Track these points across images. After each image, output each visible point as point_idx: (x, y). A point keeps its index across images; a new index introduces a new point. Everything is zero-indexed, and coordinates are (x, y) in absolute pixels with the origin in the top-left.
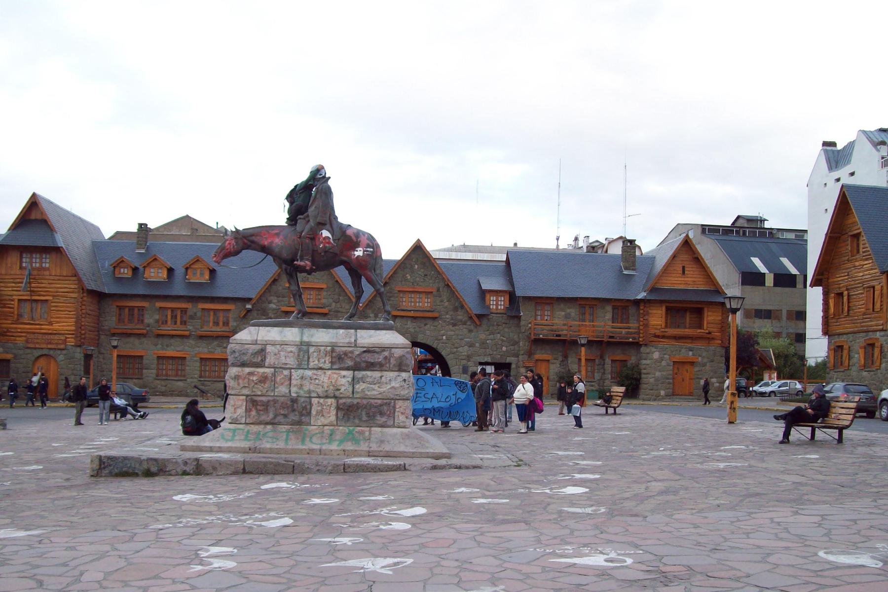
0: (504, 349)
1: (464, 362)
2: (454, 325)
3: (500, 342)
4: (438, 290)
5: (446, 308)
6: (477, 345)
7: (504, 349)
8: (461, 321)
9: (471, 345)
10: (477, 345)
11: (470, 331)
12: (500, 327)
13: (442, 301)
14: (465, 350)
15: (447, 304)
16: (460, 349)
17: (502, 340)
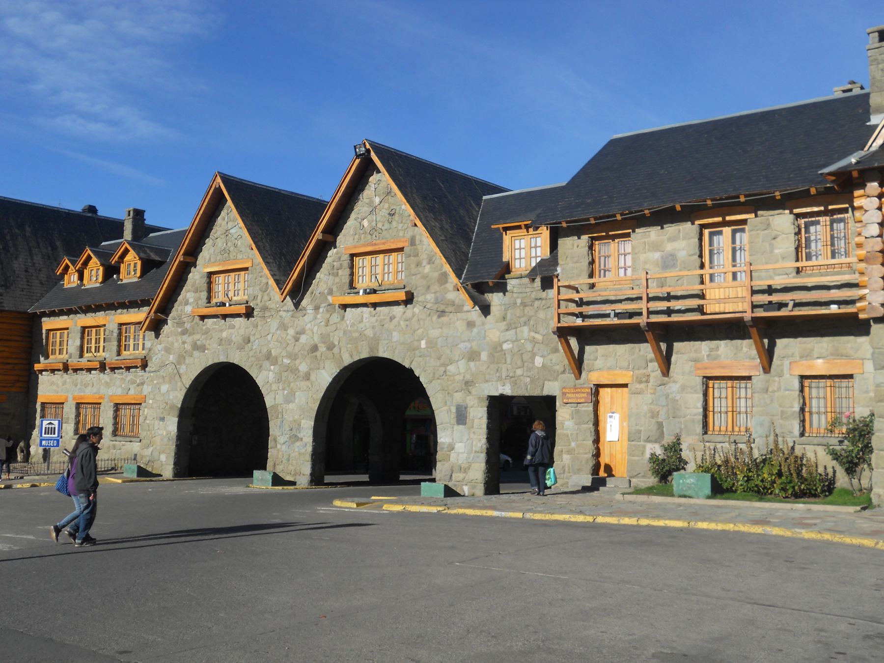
0: (539, 361)
1: (458, 397)
2: (442, 313)
3: (529, 347)
4: (413, 242)
5: (425, 277)
6: (484, 356)
7: (539, 361)
8: (453, 304)
9: (473, 356)
10: (484, 356)
11: (471, 325)
12: (529, 311)
13: (418, 264)
14: (460, 369)
15: (427, 269)
16: (452, 368)
17: (534, 341)
